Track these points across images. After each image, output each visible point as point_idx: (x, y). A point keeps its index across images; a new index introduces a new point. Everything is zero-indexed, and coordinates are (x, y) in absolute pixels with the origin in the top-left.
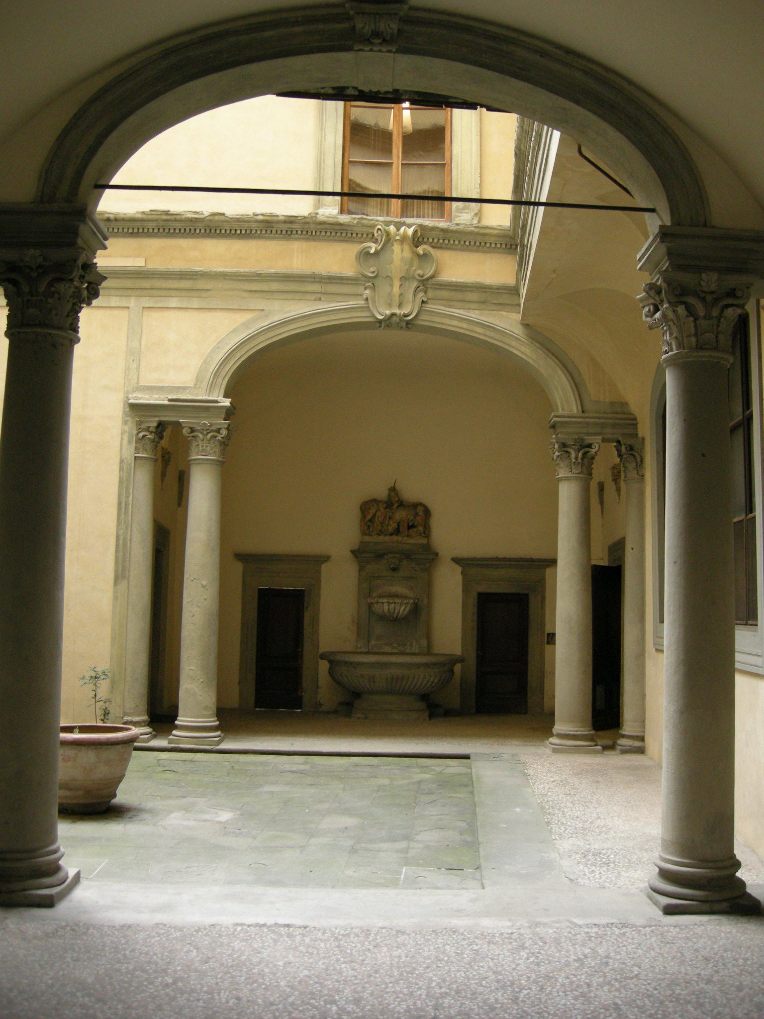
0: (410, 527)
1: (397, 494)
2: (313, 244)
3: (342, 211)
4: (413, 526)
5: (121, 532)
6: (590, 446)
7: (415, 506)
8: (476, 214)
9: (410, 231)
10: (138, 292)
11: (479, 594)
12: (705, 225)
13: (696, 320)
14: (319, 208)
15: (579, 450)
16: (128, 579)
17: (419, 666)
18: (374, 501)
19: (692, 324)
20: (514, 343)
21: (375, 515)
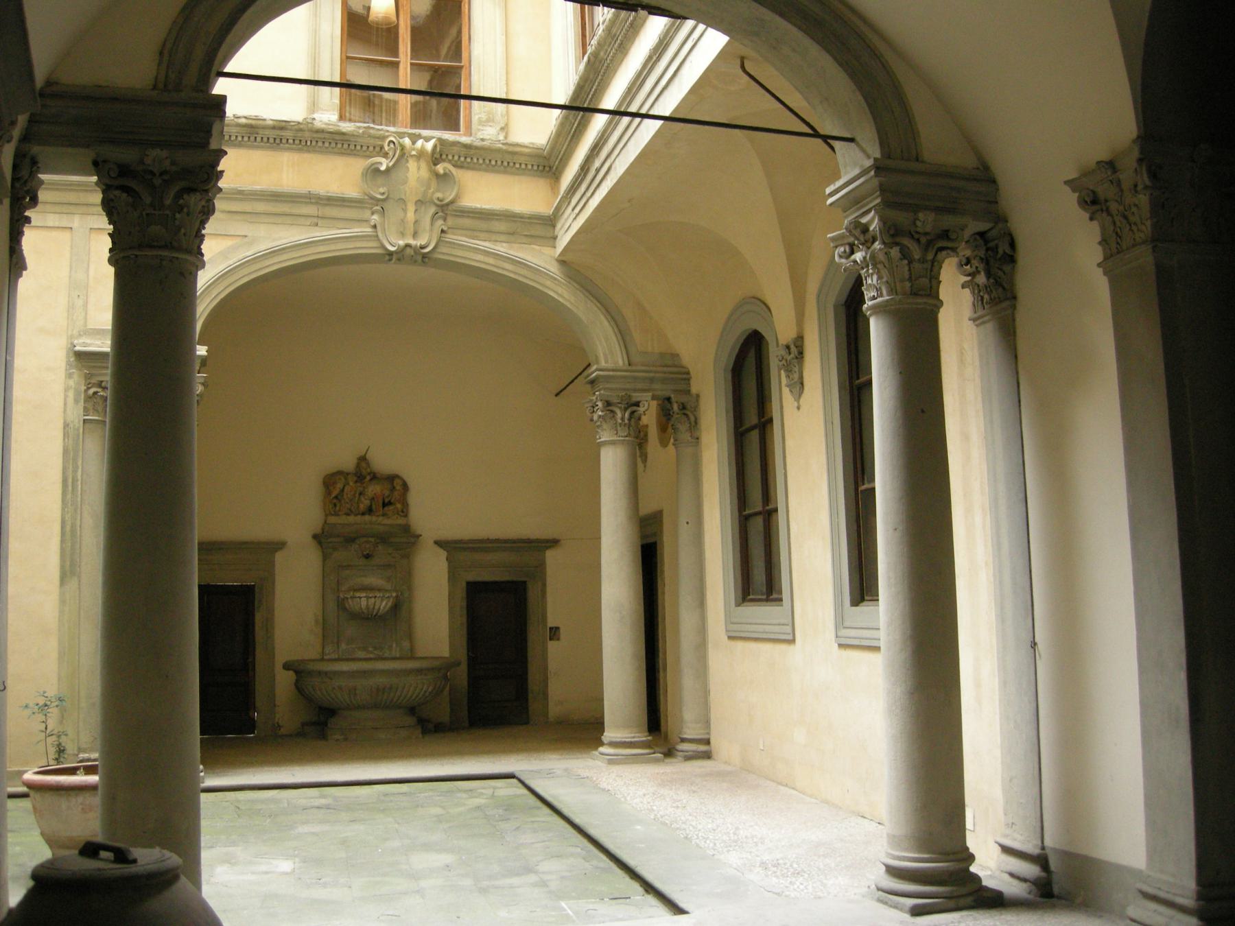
1: (368, 464)
2: (306, 156)
3: (342, 118)
4: (390, 503)
5: (68, 517)
6: (637, 404)
7: (392, 478)
8: (502, 129)
9: (429, 146)
10: (84, 209)
11: (468, 583)
12: (917, 160)
13: (910, 263)
14: (313, 112)
15: (626, 409)
16: (79, 577)
17: (408, 672)
18: (340, 473)
19: (907, 268)
20: (548, 283)
21: (343, 490)
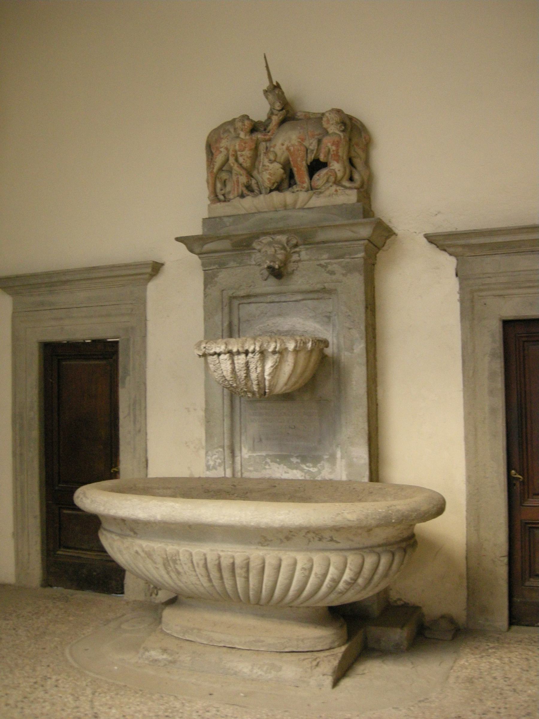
0: (315, 166)
11: (508, 324)
17: (286, 536)
